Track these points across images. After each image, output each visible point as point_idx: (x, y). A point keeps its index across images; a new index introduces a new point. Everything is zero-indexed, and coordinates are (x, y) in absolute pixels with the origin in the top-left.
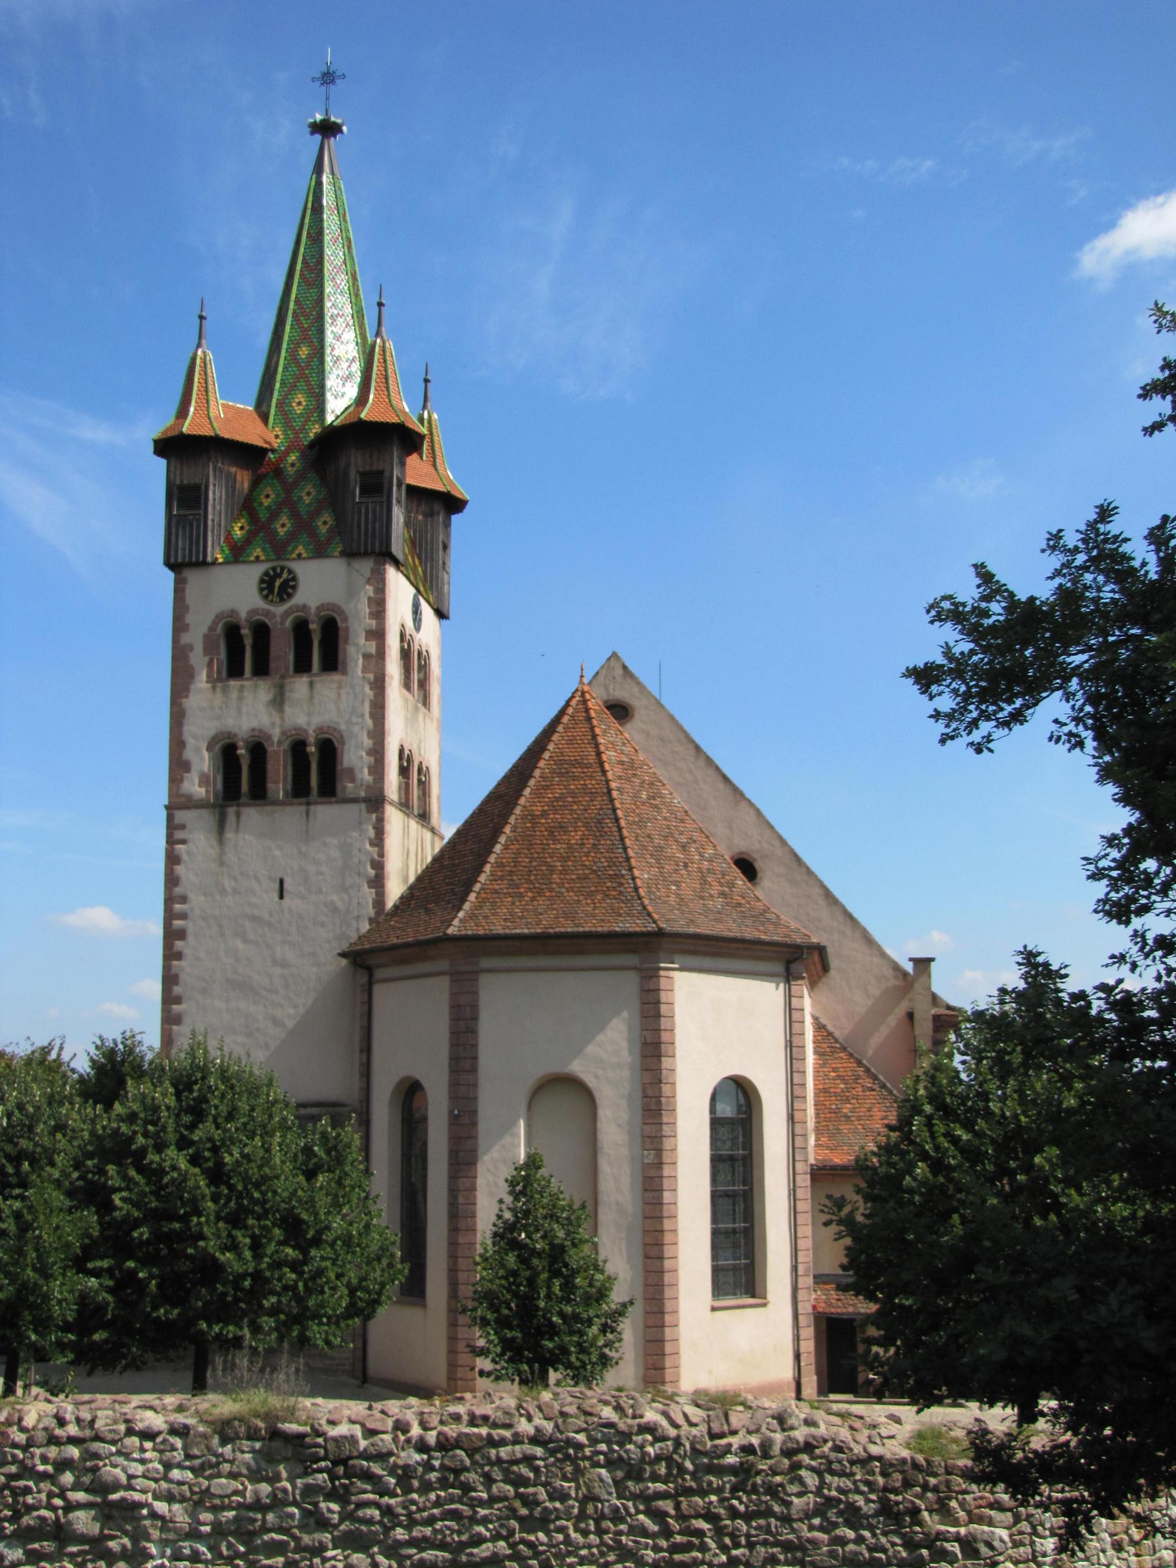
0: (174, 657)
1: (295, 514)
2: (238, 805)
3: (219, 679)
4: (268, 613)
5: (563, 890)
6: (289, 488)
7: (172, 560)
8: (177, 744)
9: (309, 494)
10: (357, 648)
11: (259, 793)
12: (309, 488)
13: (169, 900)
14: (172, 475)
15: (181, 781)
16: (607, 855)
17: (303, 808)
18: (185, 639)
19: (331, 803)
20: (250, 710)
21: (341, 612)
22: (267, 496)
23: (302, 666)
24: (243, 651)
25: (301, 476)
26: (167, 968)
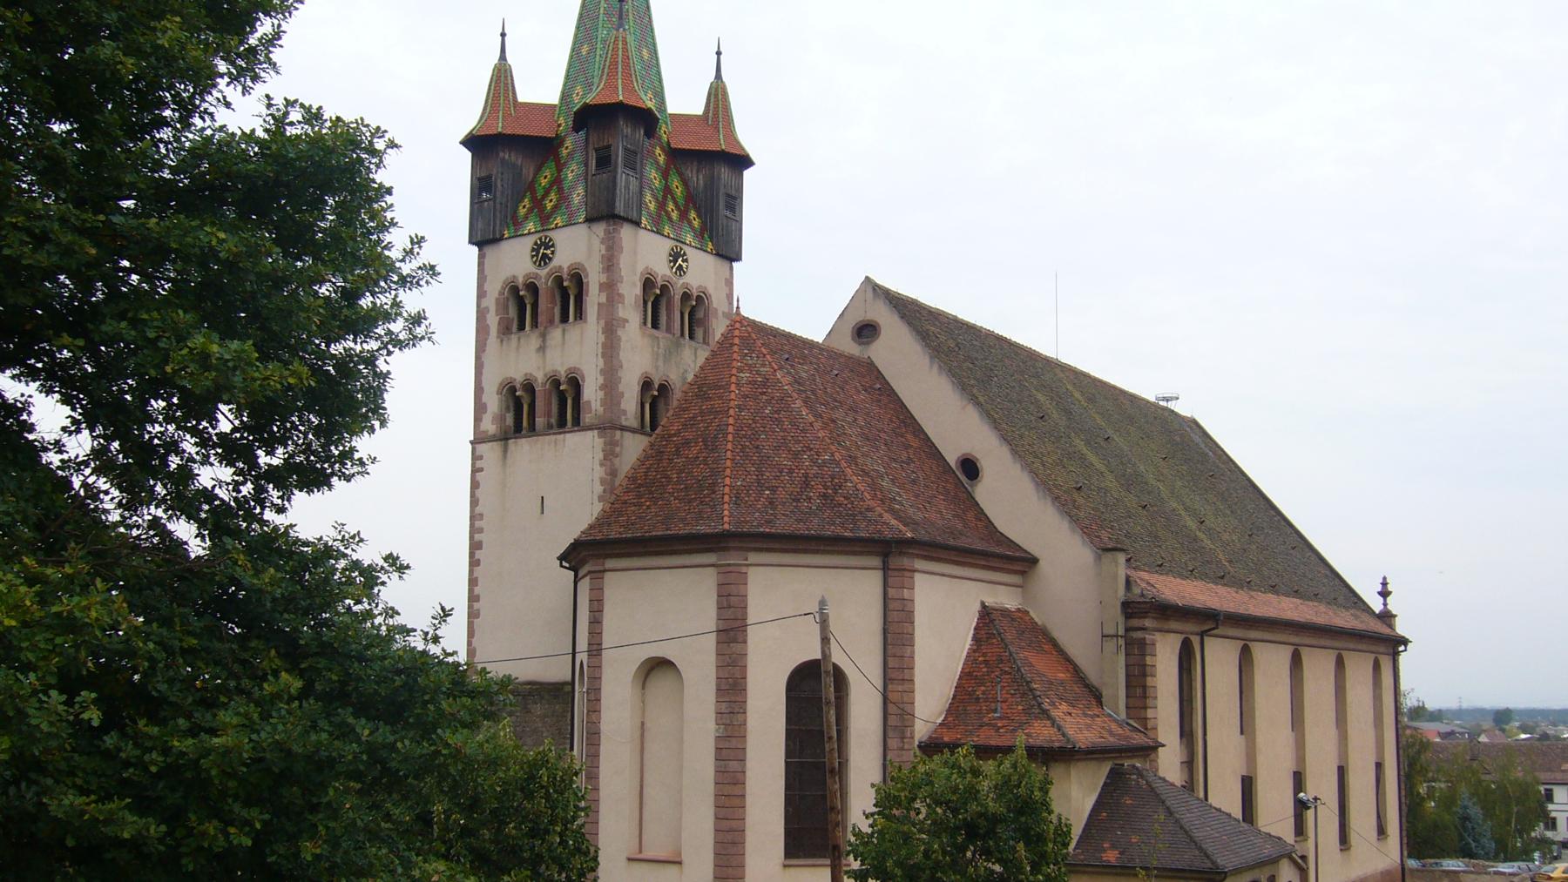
4: (537, 276)
8: (479, 390)
10: (594, 298)
13: (473, 518)
18: (485, 303)
26: (471, 572)
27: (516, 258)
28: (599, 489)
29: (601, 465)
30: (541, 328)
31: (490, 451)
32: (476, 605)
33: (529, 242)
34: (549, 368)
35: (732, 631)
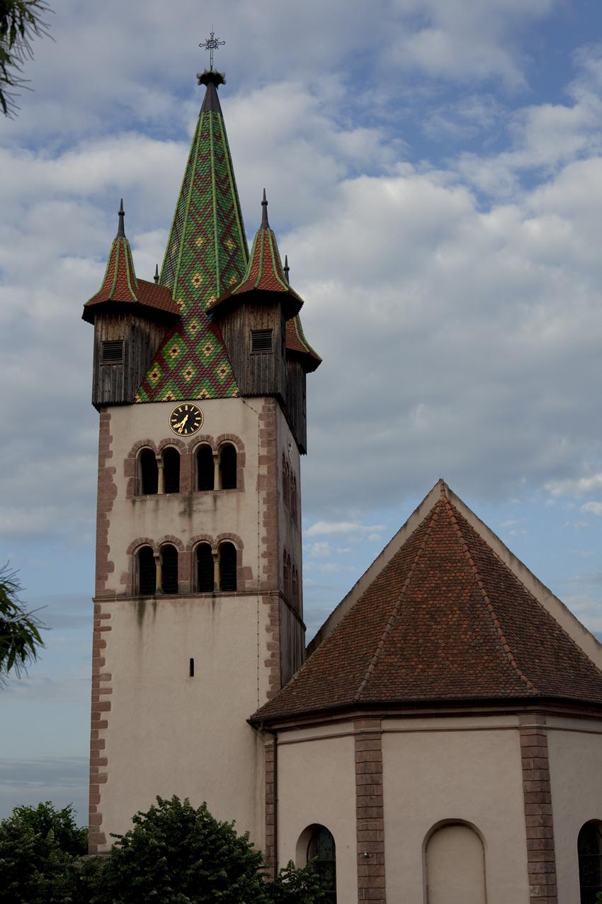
0: (99, 478)
1: (198, 364)
2: (154, 598)
3: (136, 494)
4: (178, 442)
5: (448, 663)
6: (192, 345)
7: (99, 400)
8: (102, 548)
9: (208, 349)
10: (252, 468)
11: (171, 588)
12: (208, 344)
13: (96, 678)
14: (99, 333)
15: (106, 578)
16: (481, 633)
17: (210, 600)
18: (109, 463)
19: (233, 595)
20: (164, 521)
21: (239, 442)
22: (174, 351)
23: (205, 484)
24: (155, 471)
25: (201, 336)
26: (94, 734)
27: (151, 423)
28: (266, 654)
29: (268, 630)
30: (184, 493)
31: (121, 613)
32: (102, 770)
34: (197, 533)
35: (538, 796)
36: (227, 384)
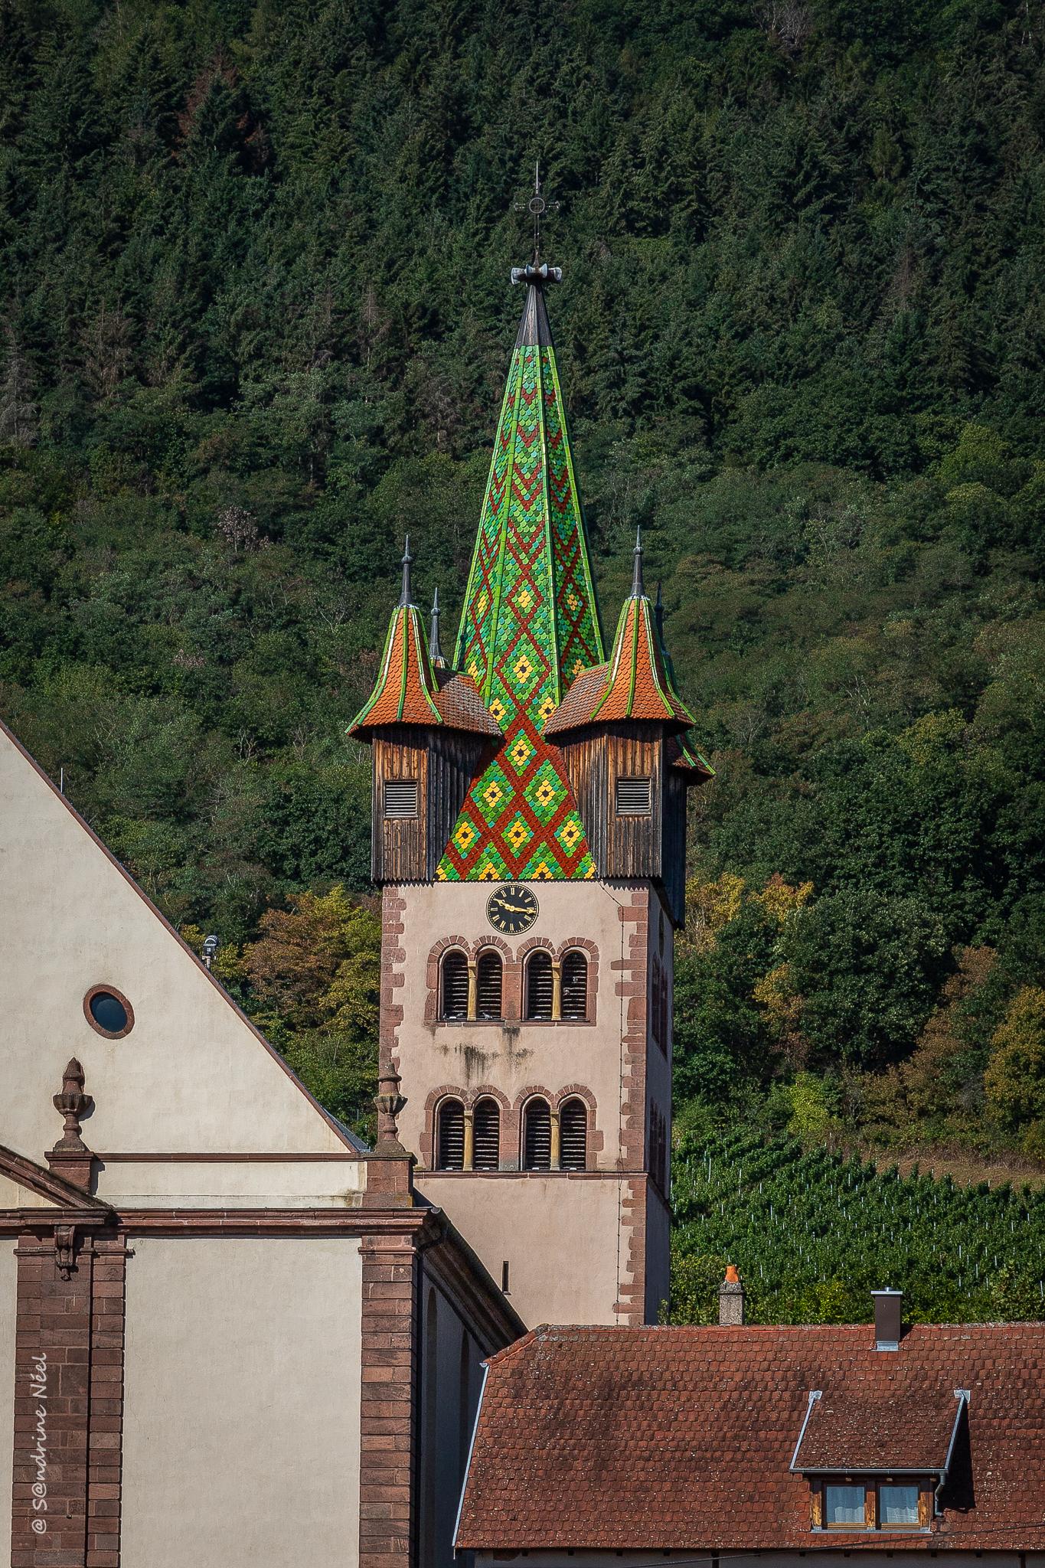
6: (519, 782)
23: (535, 1008)
33: (486, 891)
36: (579, 855)
